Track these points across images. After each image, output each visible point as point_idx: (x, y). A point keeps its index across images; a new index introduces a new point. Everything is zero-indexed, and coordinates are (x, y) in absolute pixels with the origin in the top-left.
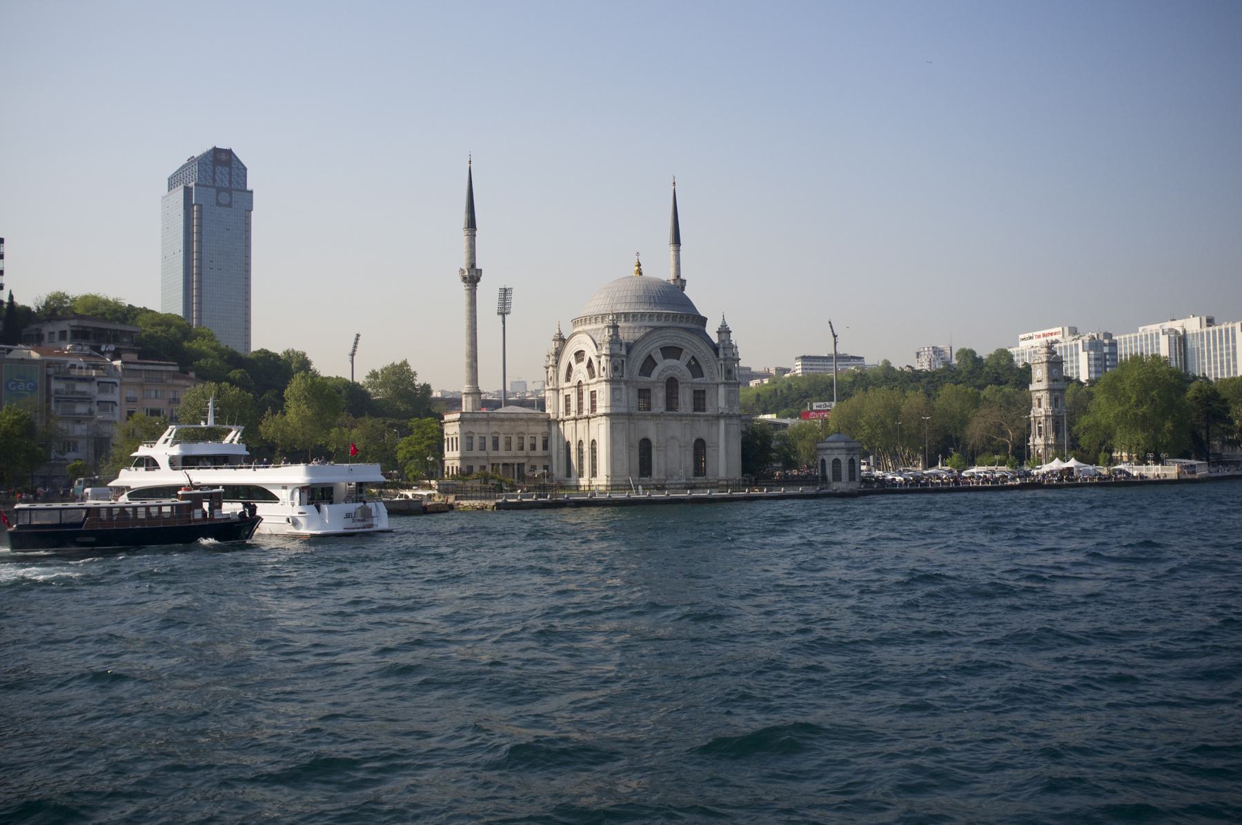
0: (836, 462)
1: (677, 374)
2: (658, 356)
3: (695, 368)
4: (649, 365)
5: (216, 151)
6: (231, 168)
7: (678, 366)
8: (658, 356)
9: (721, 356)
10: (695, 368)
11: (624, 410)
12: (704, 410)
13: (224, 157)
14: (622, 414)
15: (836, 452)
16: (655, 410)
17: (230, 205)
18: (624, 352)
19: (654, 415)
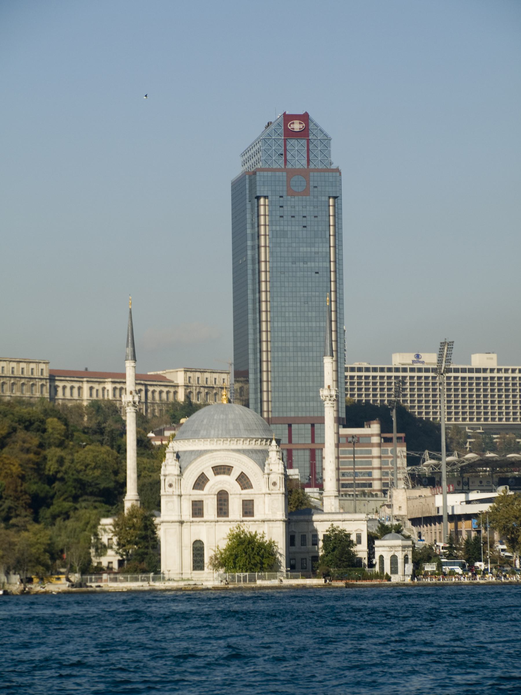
0: (381, 557)
1: (226, 488)
2: (210, 474)
3: (243, 481)
4: (201, 482)
5: (288, 118)
6: (308, 140)
7: (228, 483)
8: (210, 474)
9: (266, 471)
10: (243, 481)
11: (177, 518)
12: (253, 515)
13: (297, 126)
14: (173, 522)
15: (380, 549)
16: (206, 518)
17: (306, 192)
18: (177, 472)
19: (205, 522)
